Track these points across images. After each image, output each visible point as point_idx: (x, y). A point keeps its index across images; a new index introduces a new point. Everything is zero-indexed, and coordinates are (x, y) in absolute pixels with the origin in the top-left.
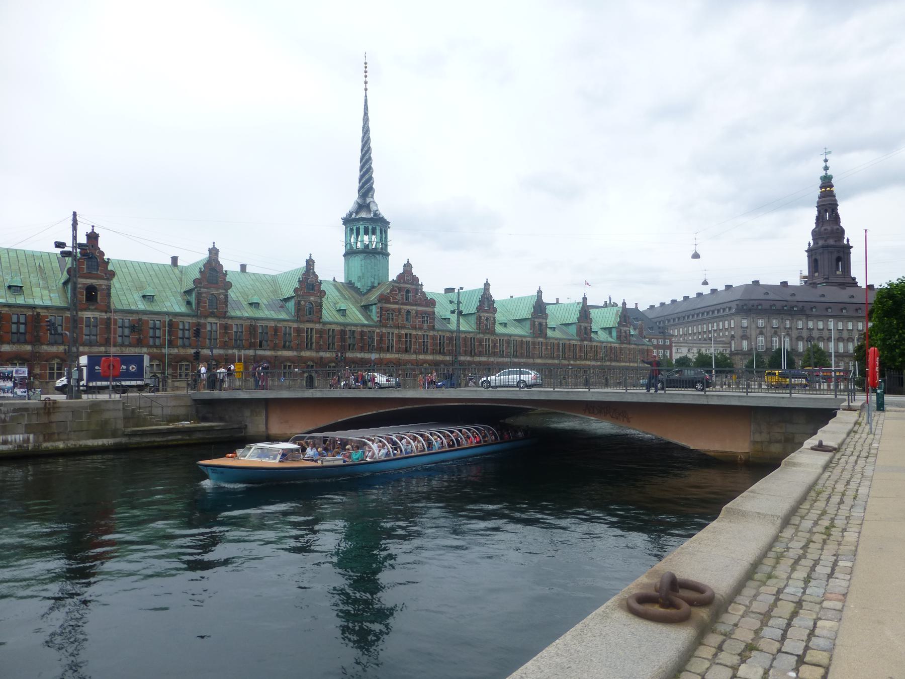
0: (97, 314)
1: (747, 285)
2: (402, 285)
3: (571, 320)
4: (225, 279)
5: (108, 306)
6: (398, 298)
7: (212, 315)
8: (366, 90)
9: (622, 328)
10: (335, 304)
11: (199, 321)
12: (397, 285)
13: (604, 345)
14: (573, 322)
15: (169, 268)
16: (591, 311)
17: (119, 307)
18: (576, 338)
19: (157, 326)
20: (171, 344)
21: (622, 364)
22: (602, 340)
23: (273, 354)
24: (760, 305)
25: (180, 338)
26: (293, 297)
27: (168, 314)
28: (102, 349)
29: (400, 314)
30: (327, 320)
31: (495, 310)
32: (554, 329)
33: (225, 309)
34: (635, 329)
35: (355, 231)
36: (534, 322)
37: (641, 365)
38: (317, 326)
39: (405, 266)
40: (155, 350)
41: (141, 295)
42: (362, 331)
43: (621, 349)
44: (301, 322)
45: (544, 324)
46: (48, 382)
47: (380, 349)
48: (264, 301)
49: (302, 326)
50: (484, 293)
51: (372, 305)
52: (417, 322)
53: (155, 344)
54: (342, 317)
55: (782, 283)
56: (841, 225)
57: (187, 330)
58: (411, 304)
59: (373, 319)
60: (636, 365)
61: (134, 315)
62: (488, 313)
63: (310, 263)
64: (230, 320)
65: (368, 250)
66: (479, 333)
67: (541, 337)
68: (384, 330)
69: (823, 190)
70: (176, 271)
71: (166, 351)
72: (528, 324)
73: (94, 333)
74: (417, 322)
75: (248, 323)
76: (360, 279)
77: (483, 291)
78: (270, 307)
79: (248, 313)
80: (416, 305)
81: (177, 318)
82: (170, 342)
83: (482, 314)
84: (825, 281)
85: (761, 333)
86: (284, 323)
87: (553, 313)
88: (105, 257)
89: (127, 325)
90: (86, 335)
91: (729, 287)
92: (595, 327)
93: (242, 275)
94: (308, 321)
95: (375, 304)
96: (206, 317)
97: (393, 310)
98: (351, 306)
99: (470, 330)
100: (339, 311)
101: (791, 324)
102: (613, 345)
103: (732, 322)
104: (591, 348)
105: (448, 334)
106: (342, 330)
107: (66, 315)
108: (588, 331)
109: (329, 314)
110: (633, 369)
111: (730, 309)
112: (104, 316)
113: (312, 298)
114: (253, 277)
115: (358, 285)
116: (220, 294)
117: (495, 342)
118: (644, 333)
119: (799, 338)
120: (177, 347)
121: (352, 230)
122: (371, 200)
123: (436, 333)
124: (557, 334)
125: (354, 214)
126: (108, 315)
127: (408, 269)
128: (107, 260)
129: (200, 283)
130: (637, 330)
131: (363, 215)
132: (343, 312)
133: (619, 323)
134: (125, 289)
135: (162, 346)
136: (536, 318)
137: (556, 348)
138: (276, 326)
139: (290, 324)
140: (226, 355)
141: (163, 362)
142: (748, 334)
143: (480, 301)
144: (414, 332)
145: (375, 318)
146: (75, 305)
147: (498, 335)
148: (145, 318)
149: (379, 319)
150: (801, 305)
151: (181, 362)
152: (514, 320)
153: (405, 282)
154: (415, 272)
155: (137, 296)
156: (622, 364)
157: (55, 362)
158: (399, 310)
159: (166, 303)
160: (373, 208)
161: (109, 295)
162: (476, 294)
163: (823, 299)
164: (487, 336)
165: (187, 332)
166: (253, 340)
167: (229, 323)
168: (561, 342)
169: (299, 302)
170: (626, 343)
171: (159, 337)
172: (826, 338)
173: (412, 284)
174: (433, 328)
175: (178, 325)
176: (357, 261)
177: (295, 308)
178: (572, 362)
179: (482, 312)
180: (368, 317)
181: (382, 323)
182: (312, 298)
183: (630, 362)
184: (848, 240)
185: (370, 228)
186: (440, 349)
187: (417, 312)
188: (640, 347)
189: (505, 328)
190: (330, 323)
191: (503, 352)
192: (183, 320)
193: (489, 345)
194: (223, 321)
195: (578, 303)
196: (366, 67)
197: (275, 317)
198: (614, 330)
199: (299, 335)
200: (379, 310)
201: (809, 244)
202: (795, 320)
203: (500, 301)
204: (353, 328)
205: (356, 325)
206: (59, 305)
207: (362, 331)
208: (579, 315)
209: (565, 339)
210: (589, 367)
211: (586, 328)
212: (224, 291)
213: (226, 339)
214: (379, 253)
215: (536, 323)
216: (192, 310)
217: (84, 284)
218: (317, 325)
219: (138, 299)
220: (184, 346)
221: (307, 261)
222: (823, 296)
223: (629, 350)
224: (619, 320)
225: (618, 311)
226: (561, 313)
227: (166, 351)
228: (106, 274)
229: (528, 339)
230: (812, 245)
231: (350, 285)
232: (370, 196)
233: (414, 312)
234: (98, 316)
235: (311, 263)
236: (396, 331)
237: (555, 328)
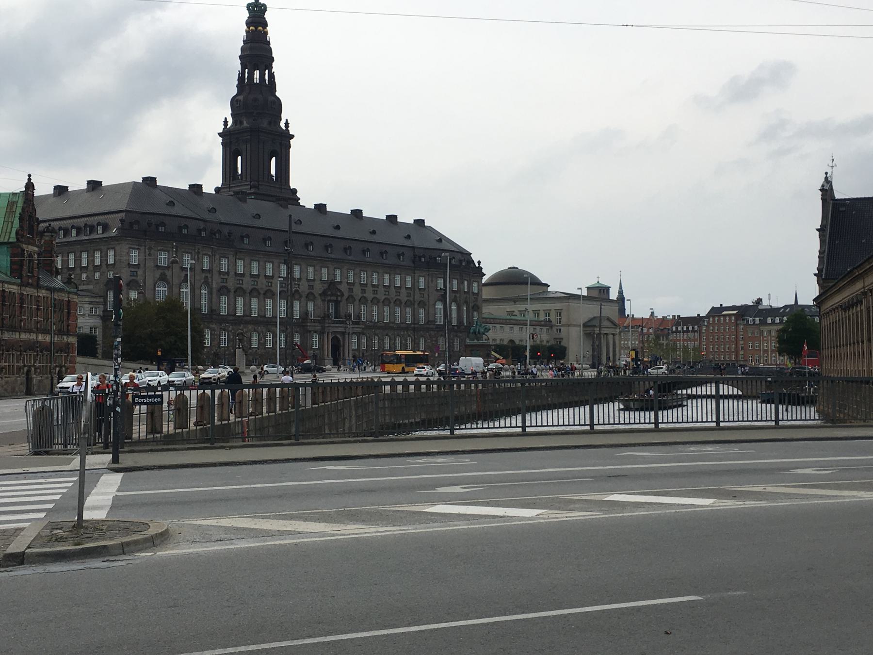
1: (135, 183)
21: (24, 336)
24: (163, 224)
55: (192, 186)
56: (277, 94)
60: (48, 339)
69: (252, 28)
84: (252, 191)
85: (163, 278)
91: (94, 185)
101: (211, 263)
103: (111, 253)
111: (106, 227)
119: (223, 290)
142: (140, 279)
150: (226, 230)
156: (24, 336)
163: (258, 223)
172: (262, 292)
183: (38, 331)
184: (287, 124)
201: (226, 122)
202: (217, 256)
222: (258, 216)
230: (230, 124)
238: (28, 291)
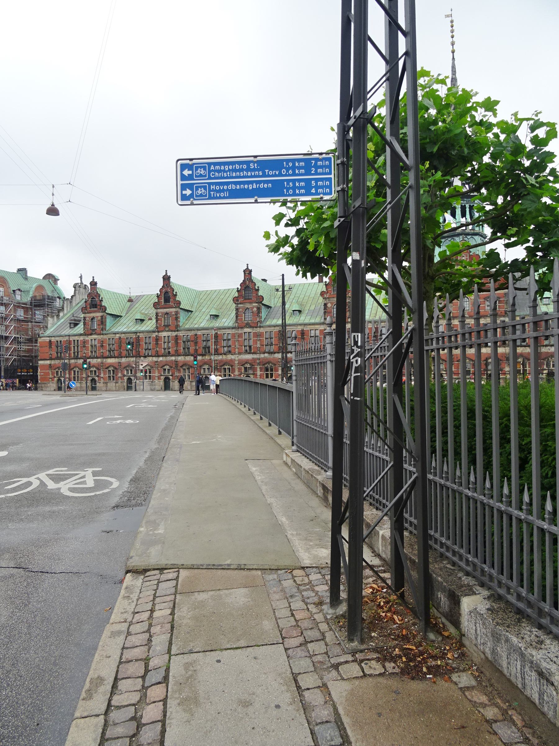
0: (169, 334)
4: (257, 294)
5: (177, 326)
8: (453, 52)
20: (217, 352)
61: (193, 332)
64: (262, 329)
78: (312, 313)
86: (310, 326)
112: (174, 334)
129: (238, 301)
138: (303, 330)
139: (317, 326)
148: (199, 333)
151: (224, 365)
196: (452, 26)
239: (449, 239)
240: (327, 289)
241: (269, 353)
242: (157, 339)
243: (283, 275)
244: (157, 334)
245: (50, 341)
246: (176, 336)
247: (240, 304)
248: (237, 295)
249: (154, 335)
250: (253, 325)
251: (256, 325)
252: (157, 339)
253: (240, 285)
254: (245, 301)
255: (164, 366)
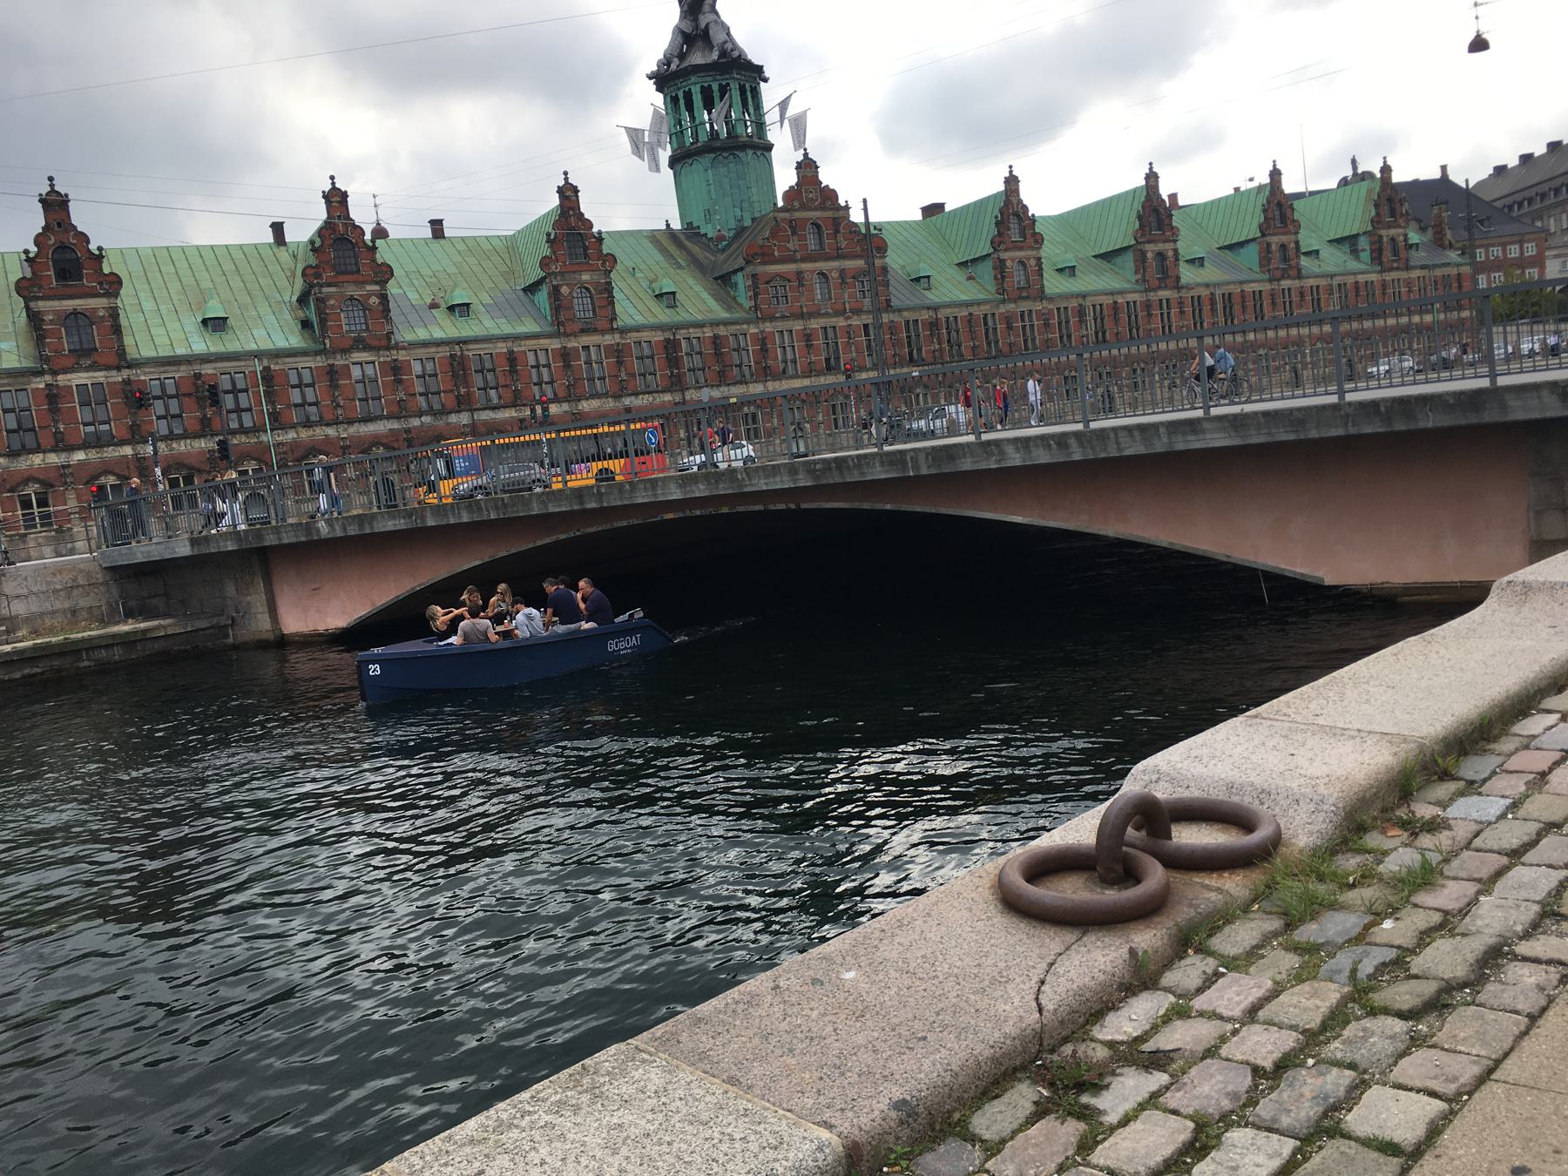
0: (100, 376)
2: (798, 215)
3: (1245, 232)
4: (374, 261)
5: (121, 352)
6: (790, 246)
7: (360, 344)
9: (1383, 232)
10: (651, 282)
11: (330, 362)
12: (786, 215)
13: (1335, 282)
14: (1251, 237)
15: (267, 253)
16: (1296, 204)
17: (147, 352)
18: (1259, 277)
19: (241, 385)
20: (278, 423)
22: (1331, 269)
23: (514, 414)
25: (296, 405)
26: (545, 278)
27: (258, 355)
28: (128, 450)
29: (801, 284)
30: (630, 322)
31: (1038, 240)
32: (1198, 262)
33: (388, 328)
34: (1423, 230)
35: (682, 102)
36: (1144, 254)
37: (1442, 316)
38: (609, 339)
39: (799, 166)
40: (244, 439)
41: (200, 320)
42: (716, 337)
43: (1384, 285)
44: (566, 335)
45: (1171, 253)
46: (25, 535)
47: (765, 373)
48: (480, 299)
49: (572, 344)
50: (1008, 203)
51: (735, 272)
52: (846, 296)
53: (241, 424)
54: (667, 311)
57: (308, 385)
58: (828, 258)
59: (741, 305)
61: (183, 368)
62: (1021, 249)
63: (568, 193)
65: (718, 144)
66: (1004, 301)
67: (1166, 288)
68: (768, 327)
70: (283, 254)
71: (267, 438)
72: (1128, 260)
73: (102, 416)
74: (846, 296)
75: (444, 352)
76: (708, 215)
77: (1004, 198)
78: (496, 309)
79: (445, 328)
80: (839, 257)
81: (279, 361)
82: (274, 416)
83: (1004, 255)
86: (528, 342)
87: (1200, 225)
88: (93, 247)
89: (171, 390)
90: (85, 424)
92: (1308, 240)
93: (436, 245)
94: (584, 331)
95: (741, 269)
96: (346, 351)
97: (784, 277)
98: (691, 281)
99: (982, 296)
100: (659, 296)
102: (1361, 278)
104: (1302, 294)
105: (925, 315)
106: (667, 340)
107: (34, 386)
108: (1292, 253)
109: (633, 307)
110: (1421, 328)
112: (117, 377)
113: (585, 277)
114: (461, 247)
115: (709, 230)
116: (369, 295)
117: (1045, 318)
118: (1449, 235)
120: (293, 426)
121: (675, 100)
122: (712, 17)
123: (895, 317)
124: (1210, 274)
125: (676, 61)
126: (125, 373)
127: (809, 173)
128: (97, 253)
129: (318, 276)
130: (1430, 232)
131: (697, 58)
132: (668, 298)
133: (1376, 222)
134: (164, 312)
135: (257, 429)
136: (1149, 242)
137: (1206, 308)
138: (511, 352)
139: (544, 342)
140: (408, 431)
141: (266, 464)
143: (997, 224)
144: (841, 322)
145: (744, 300)
146: (43, 359)
147: (1051, 299)
148: (208, 369)
149: (753, 303)
151: (306, 457)
152: (1095, 257)
153: (803, 207)
154: (826, 177)
155: (191, 323)
157: (31, 490)
158: (799, 273)
159: (255, 332)
160: (717, 37)
161: (117, 330)
162: (990, 208)
164: (1025, 306)
165: (309, 392)
166: (463, 391)
167: (400, 358)
168: (1218, 292)
169: (556, 289)
170: (1398, 269)
171: (249, 410)
173: (822, 208)
174: (888, 306)
175: (287, 376)
176: (698, 170)
177: (550, 304)
178: (1251, 336)
179: (1006, 250)
180: (729, 303)
181: (759, 314)
182: (585, 277)
185: (715, 87)
186: (911, 354)
187: (842, 272)
188: (1438, 272)
189: (1071, 280)
190: (638, 329)
191: (1069, 336)
192: (295, 366)
193: (1032, 326)
194: (385, 357)
195: (1260, 188)
197: (507, 329)
198: (1364, 243)
199: (567, 366)
200: (750, 282)
203: (1061, 216)
204: (694, 332)
205: (700, 325)
206: (17, 365)
207: (716, 337)
208: (1262, 219)
209: (1229, 283)
210: (1299, 342)
211: (1283, 247)
212: (377, 288)
213: (402, 395)
214: (744, 147)
215: (1149, 255)
216: (315, 340)
217: (55, 312)
218: (607, 337)
219: (193, 329)
220: (308, 424)
221: (560, 191)
223: (1408, 283)
224: (1373, 213)
225: (1370, 192)
226: (1219, 221)
227: (267, 438)
228: (100, 283)
229: (1131, 297)
231: (690, 230)
232: (706, 8)
233: (835, 274)
234: (102, 380)
235: (569, 193)
236: (798, 326)
237: (1202, 258)
238: (1389, 277)
239: (725, 154)
240: (554, 252)
241: (431, 411)
242: (53, 397)
243: (865, 201)
244: (48, 378)
245: (1115, 302)
246: (127, 382)
247: (329, 285)
248: (313, 261)
249: (39, 383)
250: (375, 343)
251: (384, 343)
252: (53, 397)
253: (36, 243)
254: (341, 278)
255: (97, 477)
